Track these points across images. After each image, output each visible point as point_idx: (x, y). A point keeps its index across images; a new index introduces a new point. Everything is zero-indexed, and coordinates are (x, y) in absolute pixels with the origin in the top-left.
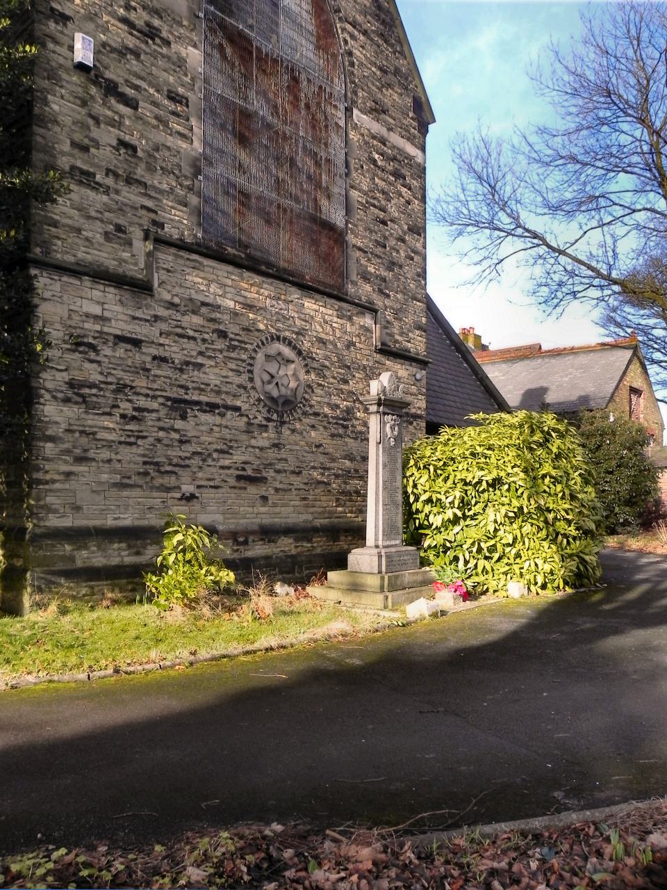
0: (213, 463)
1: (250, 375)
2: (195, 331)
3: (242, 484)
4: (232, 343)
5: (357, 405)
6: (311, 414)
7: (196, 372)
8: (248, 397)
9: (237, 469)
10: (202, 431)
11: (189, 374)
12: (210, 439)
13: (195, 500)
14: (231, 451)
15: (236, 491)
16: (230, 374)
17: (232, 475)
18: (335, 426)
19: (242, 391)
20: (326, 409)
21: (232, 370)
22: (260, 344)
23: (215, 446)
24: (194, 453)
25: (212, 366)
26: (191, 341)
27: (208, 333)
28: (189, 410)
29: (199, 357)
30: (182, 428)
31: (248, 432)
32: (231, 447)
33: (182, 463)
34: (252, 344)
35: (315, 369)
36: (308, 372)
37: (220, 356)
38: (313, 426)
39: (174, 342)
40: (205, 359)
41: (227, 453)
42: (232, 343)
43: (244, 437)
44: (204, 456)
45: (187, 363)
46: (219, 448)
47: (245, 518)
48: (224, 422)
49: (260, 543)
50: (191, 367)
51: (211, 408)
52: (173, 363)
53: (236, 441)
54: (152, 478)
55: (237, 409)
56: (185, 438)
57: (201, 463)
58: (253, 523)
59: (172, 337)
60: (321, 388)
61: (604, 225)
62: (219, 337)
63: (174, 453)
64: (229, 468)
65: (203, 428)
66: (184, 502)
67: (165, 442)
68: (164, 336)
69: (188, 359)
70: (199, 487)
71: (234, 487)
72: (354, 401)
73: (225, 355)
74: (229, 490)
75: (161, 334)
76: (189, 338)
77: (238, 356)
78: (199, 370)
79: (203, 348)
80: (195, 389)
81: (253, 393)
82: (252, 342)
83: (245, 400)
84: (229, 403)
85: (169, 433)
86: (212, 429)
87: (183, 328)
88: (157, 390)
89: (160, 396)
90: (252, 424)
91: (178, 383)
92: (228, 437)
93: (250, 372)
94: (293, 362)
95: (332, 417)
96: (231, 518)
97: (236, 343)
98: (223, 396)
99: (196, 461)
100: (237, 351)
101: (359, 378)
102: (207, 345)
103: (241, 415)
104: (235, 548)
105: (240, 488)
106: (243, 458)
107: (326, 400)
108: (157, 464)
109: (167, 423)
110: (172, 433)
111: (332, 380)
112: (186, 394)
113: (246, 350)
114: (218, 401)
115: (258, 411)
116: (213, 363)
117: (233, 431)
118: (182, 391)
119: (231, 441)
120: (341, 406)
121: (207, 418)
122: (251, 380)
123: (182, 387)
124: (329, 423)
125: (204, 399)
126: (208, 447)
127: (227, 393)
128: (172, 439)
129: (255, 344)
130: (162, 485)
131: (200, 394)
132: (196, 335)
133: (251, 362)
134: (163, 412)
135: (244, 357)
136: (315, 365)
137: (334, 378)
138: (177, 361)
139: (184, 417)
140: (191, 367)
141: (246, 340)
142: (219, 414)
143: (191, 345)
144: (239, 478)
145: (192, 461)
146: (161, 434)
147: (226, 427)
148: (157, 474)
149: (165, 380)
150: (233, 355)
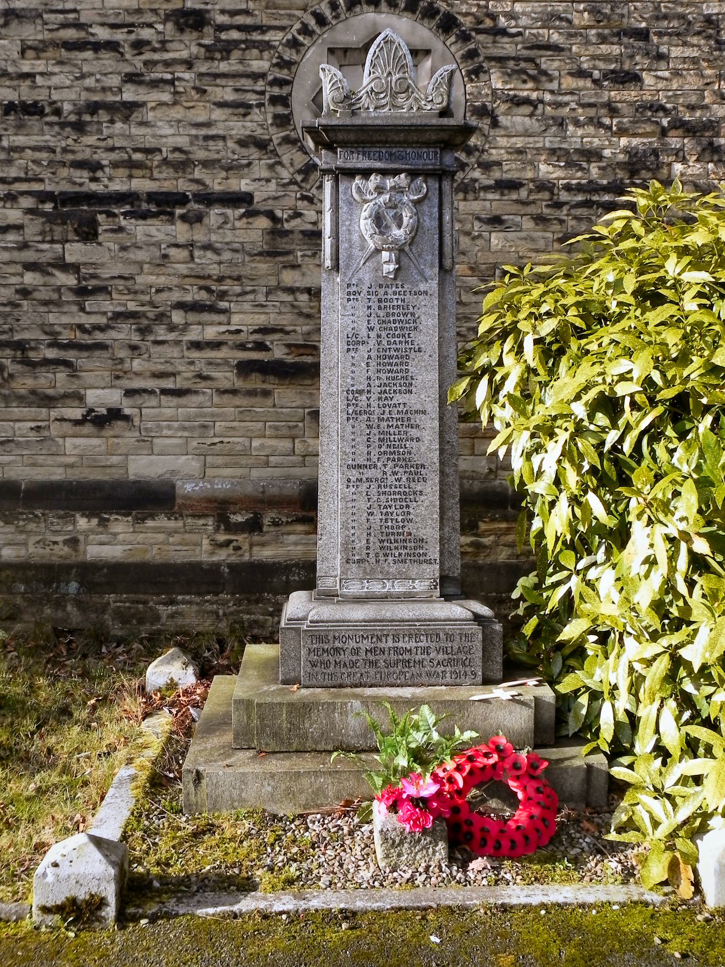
0: (171, 336)
1: (280, 110)
2: (114, 26)
3: (255, 382)
4: (224, 36)
5: (674, 141)
6: (486, 188)
7: (119, 125)
8: (271, 167)
9: (242, 347)
10: (140, 264)
11: (100, 131)
12: (162, 281)
13: (120, 423)
14: (223, 305)
15: (238, 400)
16: (218, 114)
17: (226, 362)
18: (579, 212)
19: (254, 153)
20: (543, 168)
21: (222, 105)
22: (312, 22)
23: (176, 296)
24: (117, 316)
25: (162, 104)
26: (105, 55)
27: (150, 26)
28: (101, 218)
29: (129, 86)
30: (83, 260)
31: (272, 254)
32: (223, 295)
33: (87, 339)
34: (282, 29)
35: (501, 60)
36: (476, 73)
37: (187, 76)
38: (496, 221)
39: (60, 63)
40: (142, 90)
41: (212, 309)
42: (224, 36)
43: (263, 267)
44: (145, 323)
45: (93, 108)
46: (188, 298)
47: (267, 464)
48: (199, 235)
49: (300, 528)
50: (103, 116)
51: (165, 204)
52: (58, 112)
53: (238, 278)
54: (11, 376)
55: (241, 199)
56: (94, 282)
57: (135, 338)
58: (287, 478)
59: (50, 53)
60: (527, 110)
61: (67, 241)
62: (181, 30)
63: (64, 319)
64: (216, 345)
65: (141, 255)
66: (88, 429)
67: (43, 294)
68: (30, 54)
69: (96, 98)
70: (130, 393)
71: (234, 392)
72: (664, 132)
73: (203, 69)
74: (216, 399)
75: (23, 53)
76: (97, 47)
77: (239, 68)
78: (126, 119)
79: (137, 63)
80: (115, 165)
81: (288, 155)
82: (285, 22)
83: (265, 174)
84: (217, 188)
85: (49, 274)
86: (165, 256)
87: (79, 26)
88: (17, 180)
89: (23, 193)
90: (287, 233)
91: (70, 157)
92: (214, 270)
93: (284, 101)
94: (427, 52)
95: (568, 188)
96: (226, 466)
97: (235, 35)
98: (198, 173)
99: (125, 333)
100: (236, 54)
101: (684, 60)
102: (148, 56)
103: (251, 214)
104: (222, 538)
105: (251, 393)
106: (261, 320)
107: (548, 142)
108: (21, 346)
109: (48, 251)
110: (57, 273)
111: (569, 82)
112: (94, 179)
113: (267, 46)
114: (183, 186)
115: (304, 198)
116: (166, 97)
117: (227, 256)
118: (82, 176)
119: (220, 279)
120: (607, 153)
121: (153, 230)
122: (283, 121)
123: (79, 165)
124: (558, 205)
125: (141, 185)
126: (158, 298)
127: (206, 164)
128: (58, 290)
129: (298, 26)
130: (33, 392)
131: (130, 177)
132: (119, 36)
133: (283, 74)
134: (33, 228)
135: (259, 64)
136: (507, 47)
137: (581, 74)
138: (67, 107)
139: (88, 233)
140: (103, 116)
141: (266, 21)
142: (183, 218)
143: (107, 60)
144: (245, 368)
145: (113, 334)
146: (30, 278)
147: (208, 247)
148: (19, 367)
149: (38, 155)
150: (224, 67)
